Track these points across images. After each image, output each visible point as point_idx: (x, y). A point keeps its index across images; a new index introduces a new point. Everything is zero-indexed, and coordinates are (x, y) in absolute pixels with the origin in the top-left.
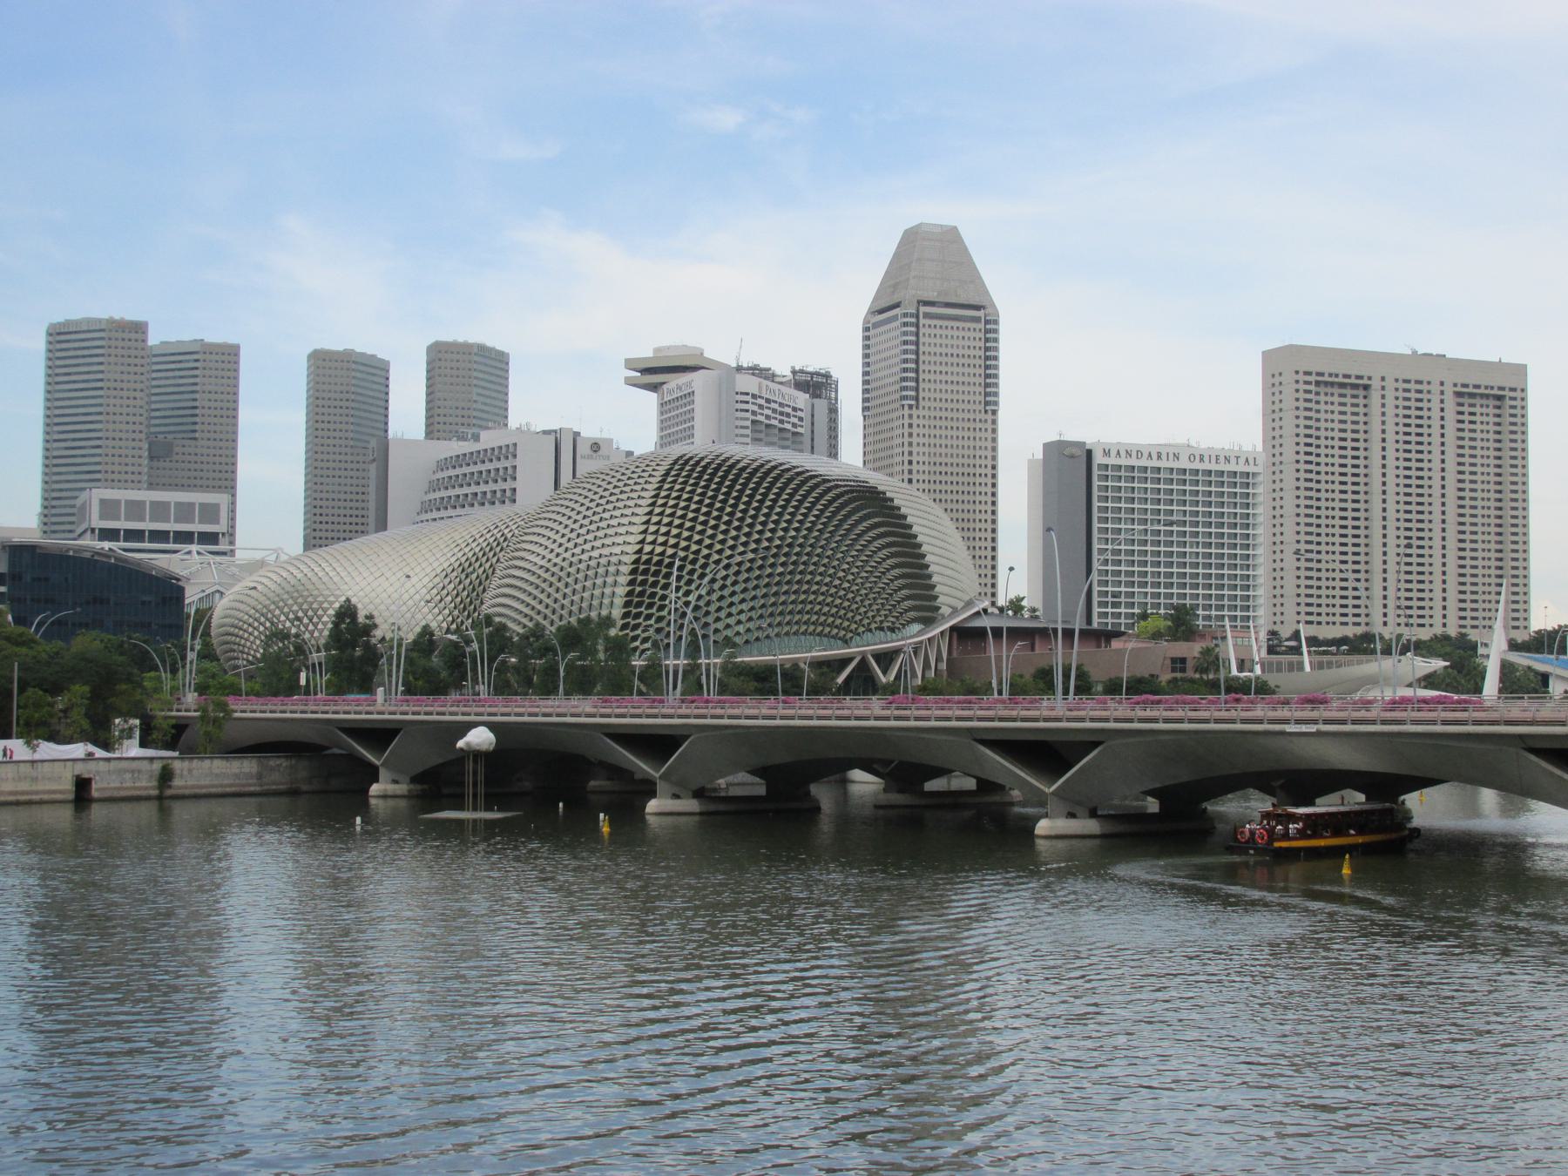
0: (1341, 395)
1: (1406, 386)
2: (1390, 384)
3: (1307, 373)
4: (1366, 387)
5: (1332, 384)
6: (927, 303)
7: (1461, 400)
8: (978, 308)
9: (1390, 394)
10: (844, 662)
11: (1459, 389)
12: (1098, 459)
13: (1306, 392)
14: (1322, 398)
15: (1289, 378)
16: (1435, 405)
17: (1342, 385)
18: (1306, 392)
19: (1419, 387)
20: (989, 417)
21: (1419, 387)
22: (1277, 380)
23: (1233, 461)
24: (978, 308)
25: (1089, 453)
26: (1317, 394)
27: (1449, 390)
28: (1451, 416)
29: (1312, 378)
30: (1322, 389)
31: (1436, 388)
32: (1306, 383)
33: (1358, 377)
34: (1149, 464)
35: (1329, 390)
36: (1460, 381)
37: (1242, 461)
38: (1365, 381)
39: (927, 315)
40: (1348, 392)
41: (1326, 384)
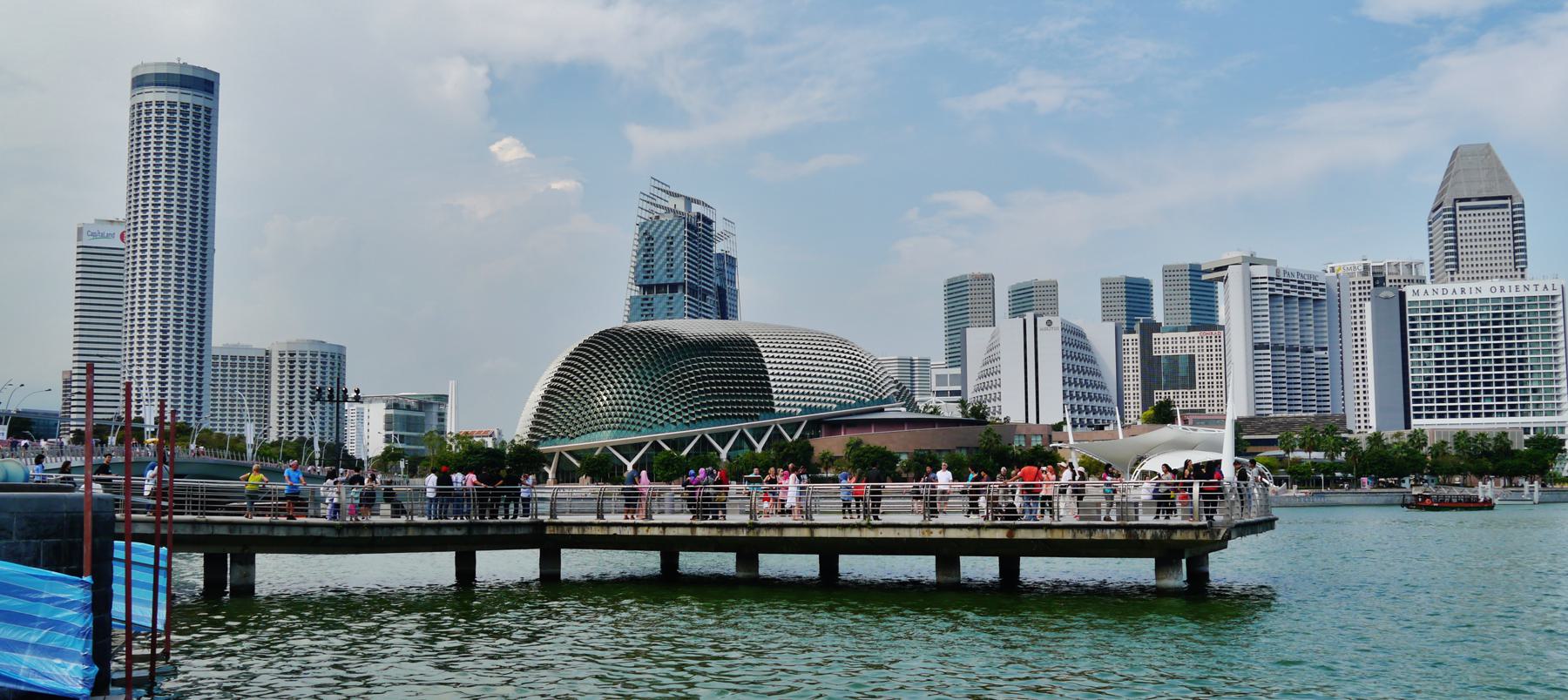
6: (1461, 200)
8: (1505, 198)
12: (1409, 298)
20: (1519, 273)
23: (1532, 288)
24: (1505, 198)
25: (1402, 295)
34: (1455, 297)
37: (1540, 288)
39: (1462, 208)
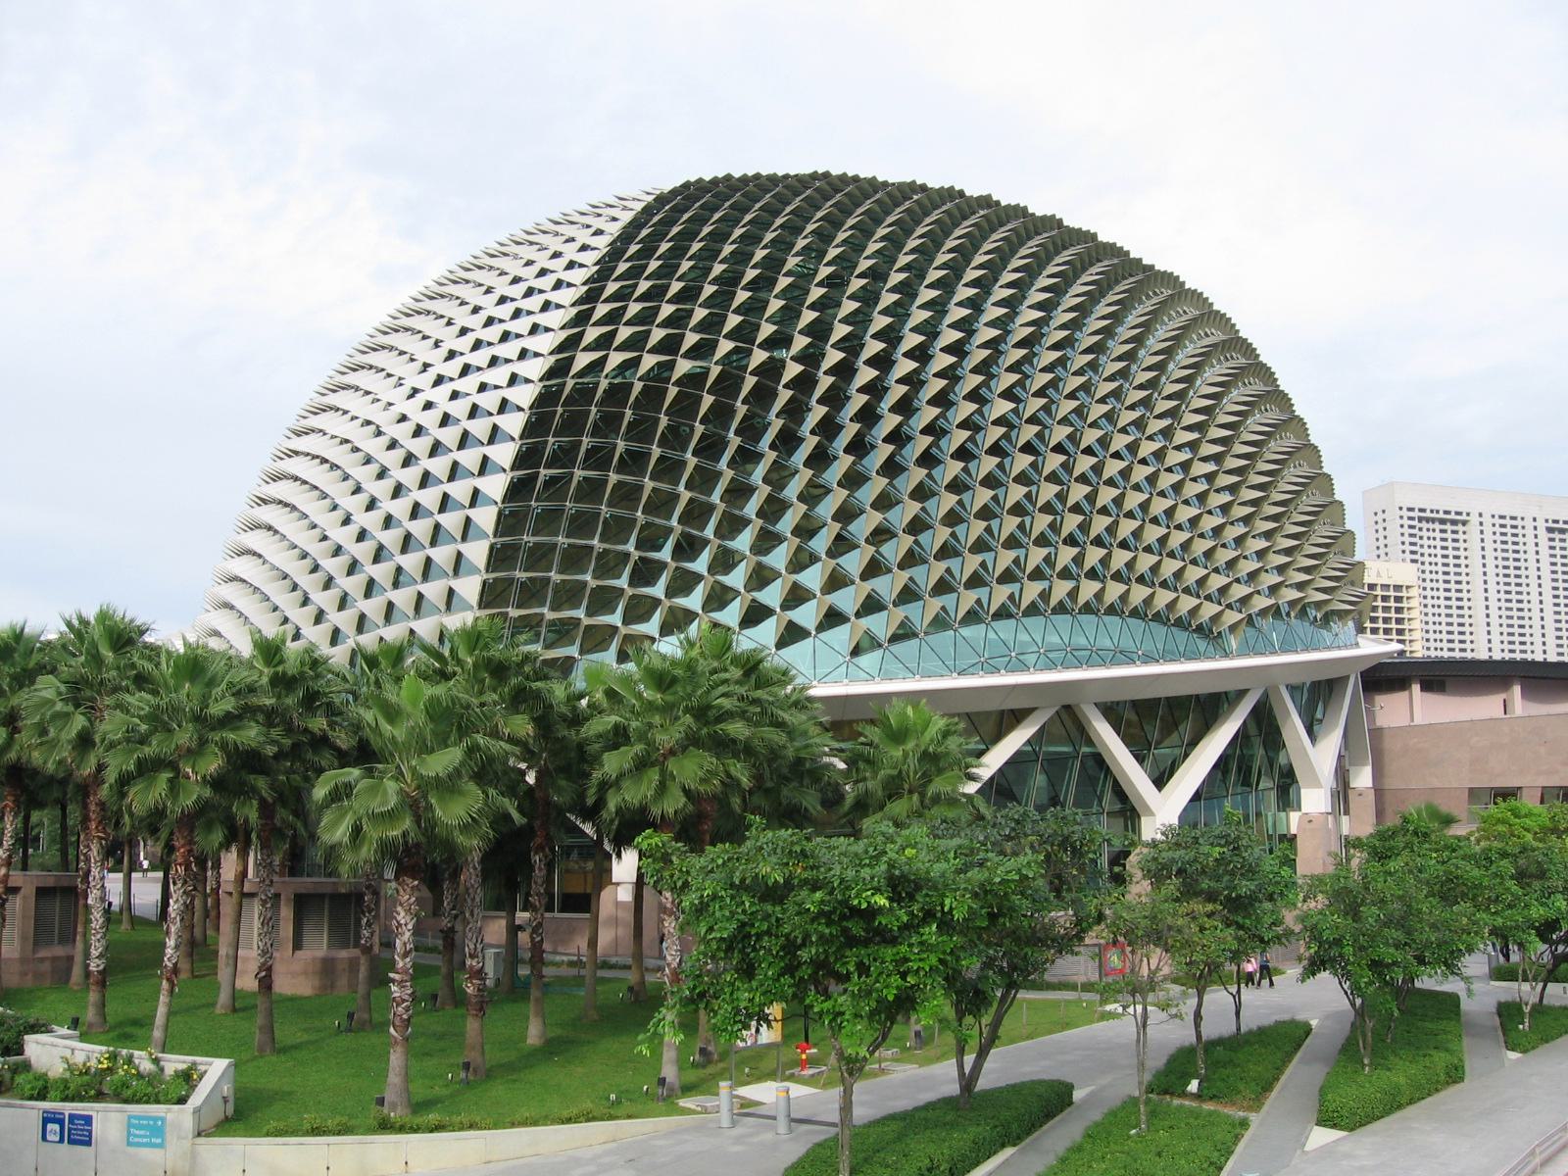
0: (1442, 531)
1: (1502, 522)
2: (1487, 520)
3: (1410, 509)
4: (1464, 523)
5: (1433, 520)
7: (1552, 536)
9: (1488, 529)
10: (1207, 708)
11: (1550, 524)
13: (1411, 527)
14: (1425, 533)
15: (1393, 515)
16: (1530, 540)
17: (1443, 522)
18: (1411, 527)
19: (1514, 523)
21: (1514, 523)
22: (1380, 518)
26: (1420, 529)
27: (1542, 526)
28: (1545, 552)
29: (1416, 514)
30: (1424, 525)
31: (1529, 524)
32: (1410, 518)
33: (1457, 513)
35: (1431, 526)
36: (1551, 518)
38: (1464, 517)
40: (1448, 527)
41: (1428, 520)
